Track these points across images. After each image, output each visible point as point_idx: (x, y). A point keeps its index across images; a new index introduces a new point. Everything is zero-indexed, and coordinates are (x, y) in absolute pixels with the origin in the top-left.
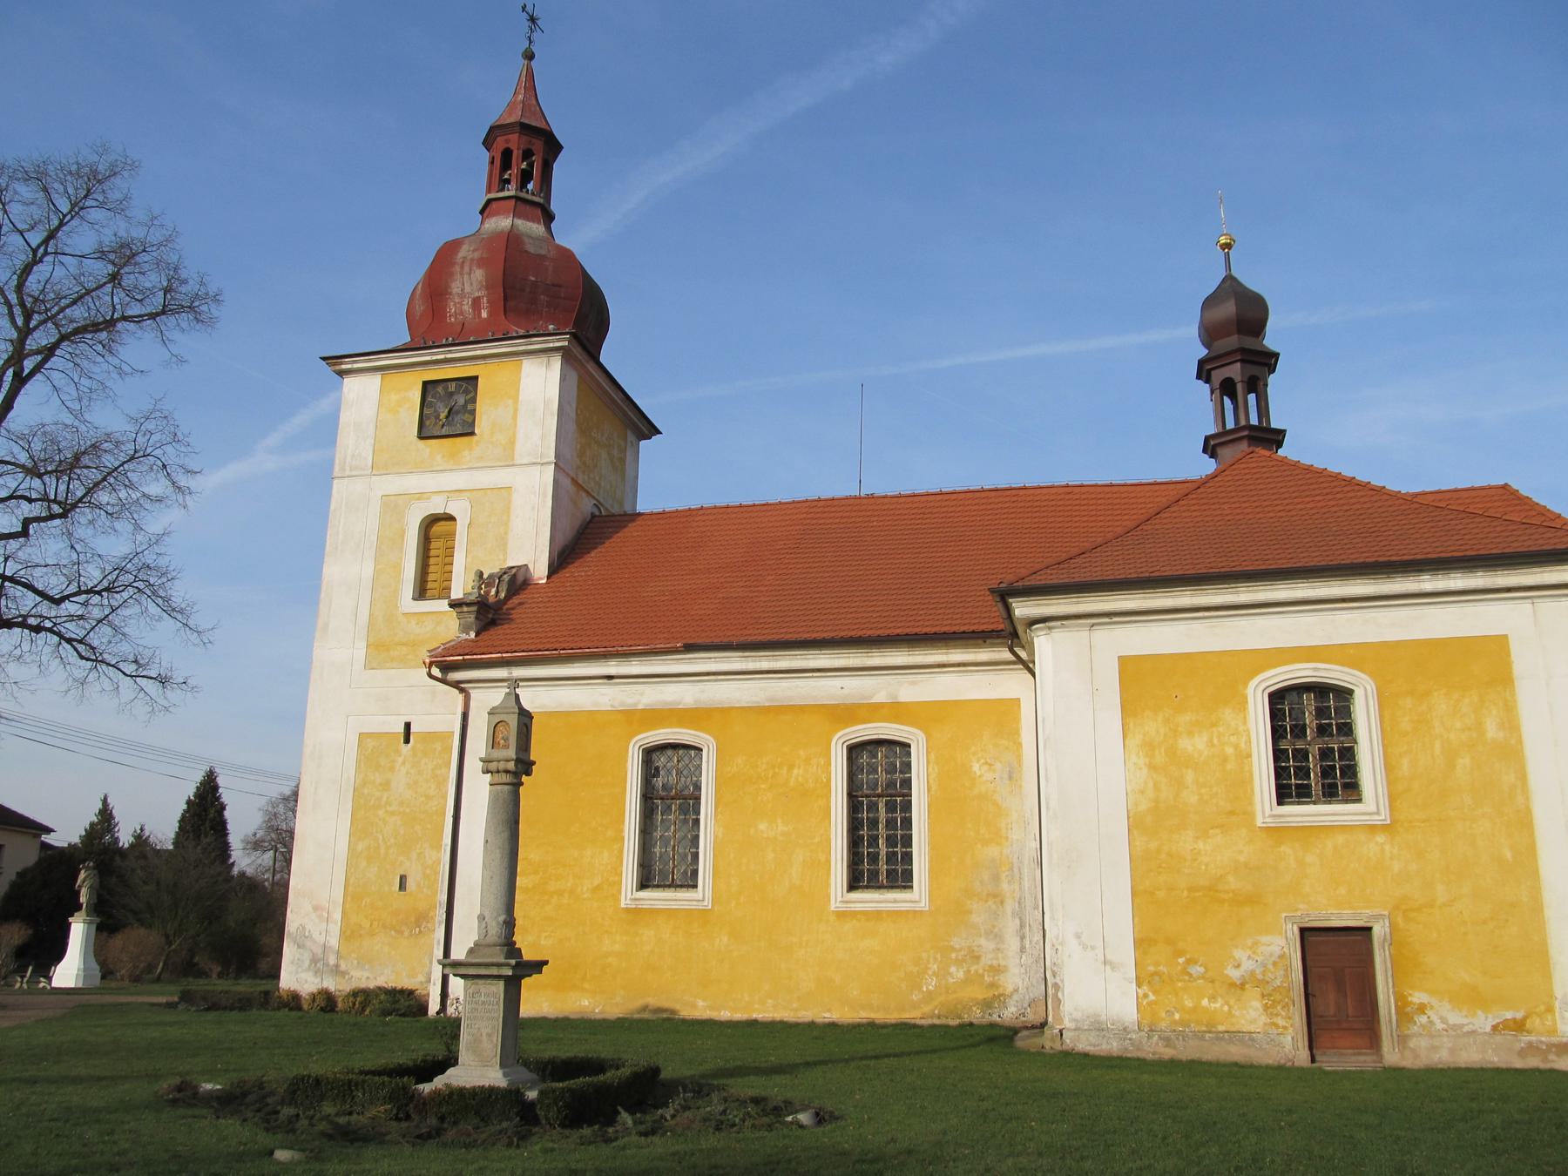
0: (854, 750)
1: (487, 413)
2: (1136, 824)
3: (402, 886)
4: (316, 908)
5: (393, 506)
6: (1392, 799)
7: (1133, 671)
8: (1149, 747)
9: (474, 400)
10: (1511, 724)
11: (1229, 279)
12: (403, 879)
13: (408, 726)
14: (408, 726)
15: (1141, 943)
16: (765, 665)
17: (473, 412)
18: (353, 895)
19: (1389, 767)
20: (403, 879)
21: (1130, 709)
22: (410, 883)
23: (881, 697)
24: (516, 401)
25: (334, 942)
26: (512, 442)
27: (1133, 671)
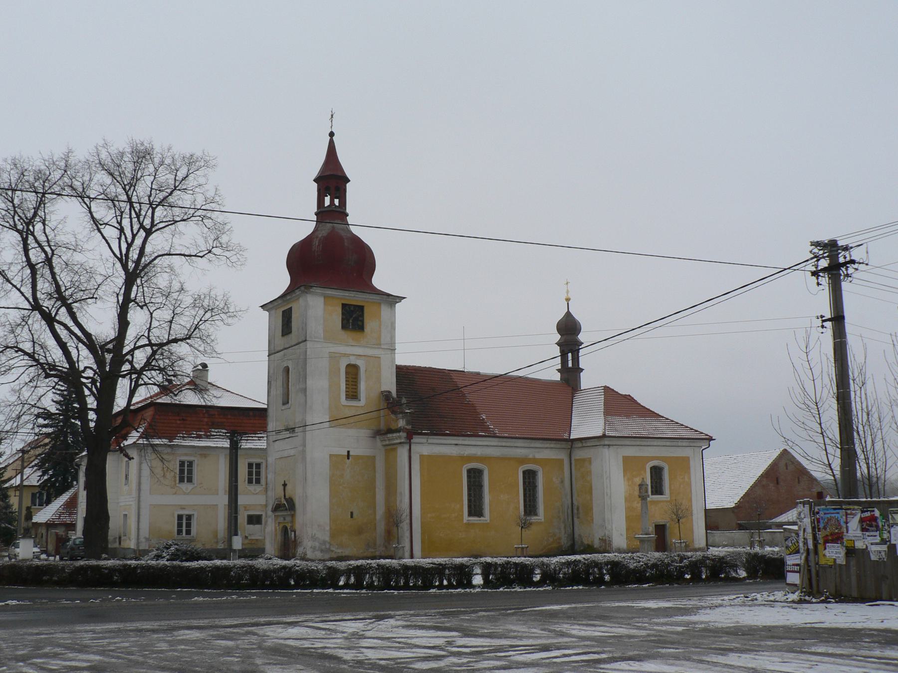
0: (524, 472)
1: (370, 325)
2: (626, 500)
3: (352, 517)
4: (319, 526)
5: (334, 358)
6: (671, 494)
7: (626, 459)
8: (628, 480)
9: (362, 315)
10: (690, 478)
11: (568, 314)
12: (352, 513)
13: (348, 452)
14: (348, 452)
15: (627, 529)
16: (504, 444)
17: (363, 321)
18: (333, 520)
19: (670, 485)
20: (352, 513)
21: (625, 471)
22: (355, 515)
23: (531, 456)
24: (380, 321)
25: (327, 539)
26: (379, 337)
27: (626, 459)
